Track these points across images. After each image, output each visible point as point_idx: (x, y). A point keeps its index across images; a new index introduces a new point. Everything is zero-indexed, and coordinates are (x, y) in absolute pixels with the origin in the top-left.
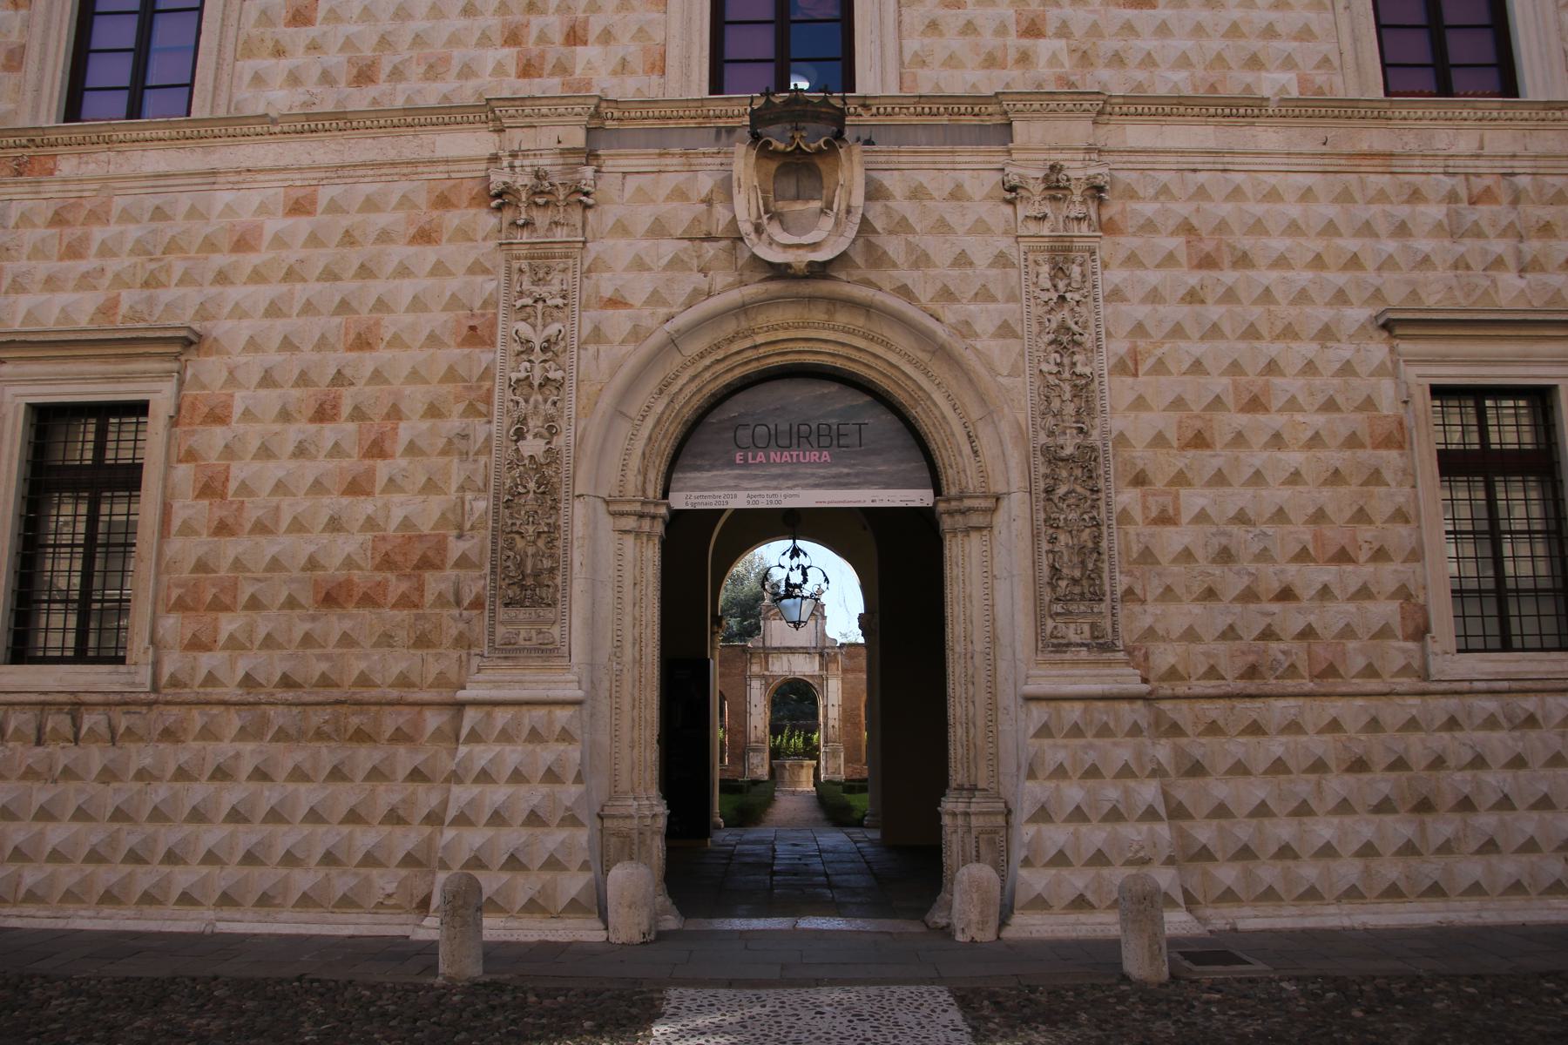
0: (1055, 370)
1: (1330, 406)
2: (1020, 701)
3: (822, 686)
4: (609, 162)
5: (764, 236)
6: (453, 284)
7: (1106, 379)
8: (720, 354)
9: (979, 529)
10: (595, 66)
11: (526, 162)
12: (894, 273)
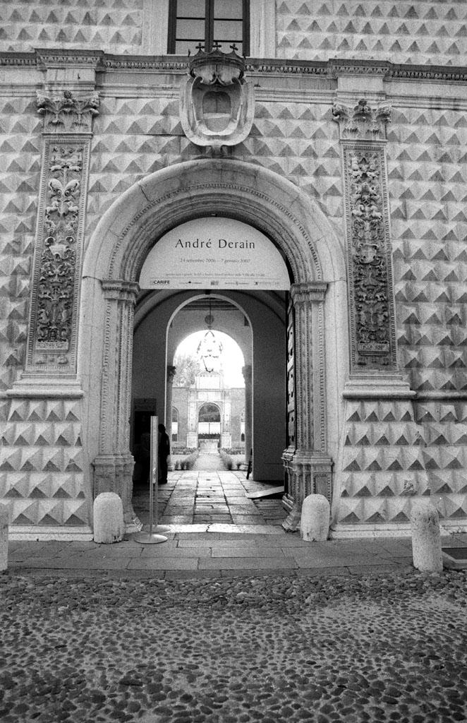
4: (108, 91)
7: (389, 219)
8: (170, 201)
9: (317, 302)
11: (60, 88)
12: (271, 158)
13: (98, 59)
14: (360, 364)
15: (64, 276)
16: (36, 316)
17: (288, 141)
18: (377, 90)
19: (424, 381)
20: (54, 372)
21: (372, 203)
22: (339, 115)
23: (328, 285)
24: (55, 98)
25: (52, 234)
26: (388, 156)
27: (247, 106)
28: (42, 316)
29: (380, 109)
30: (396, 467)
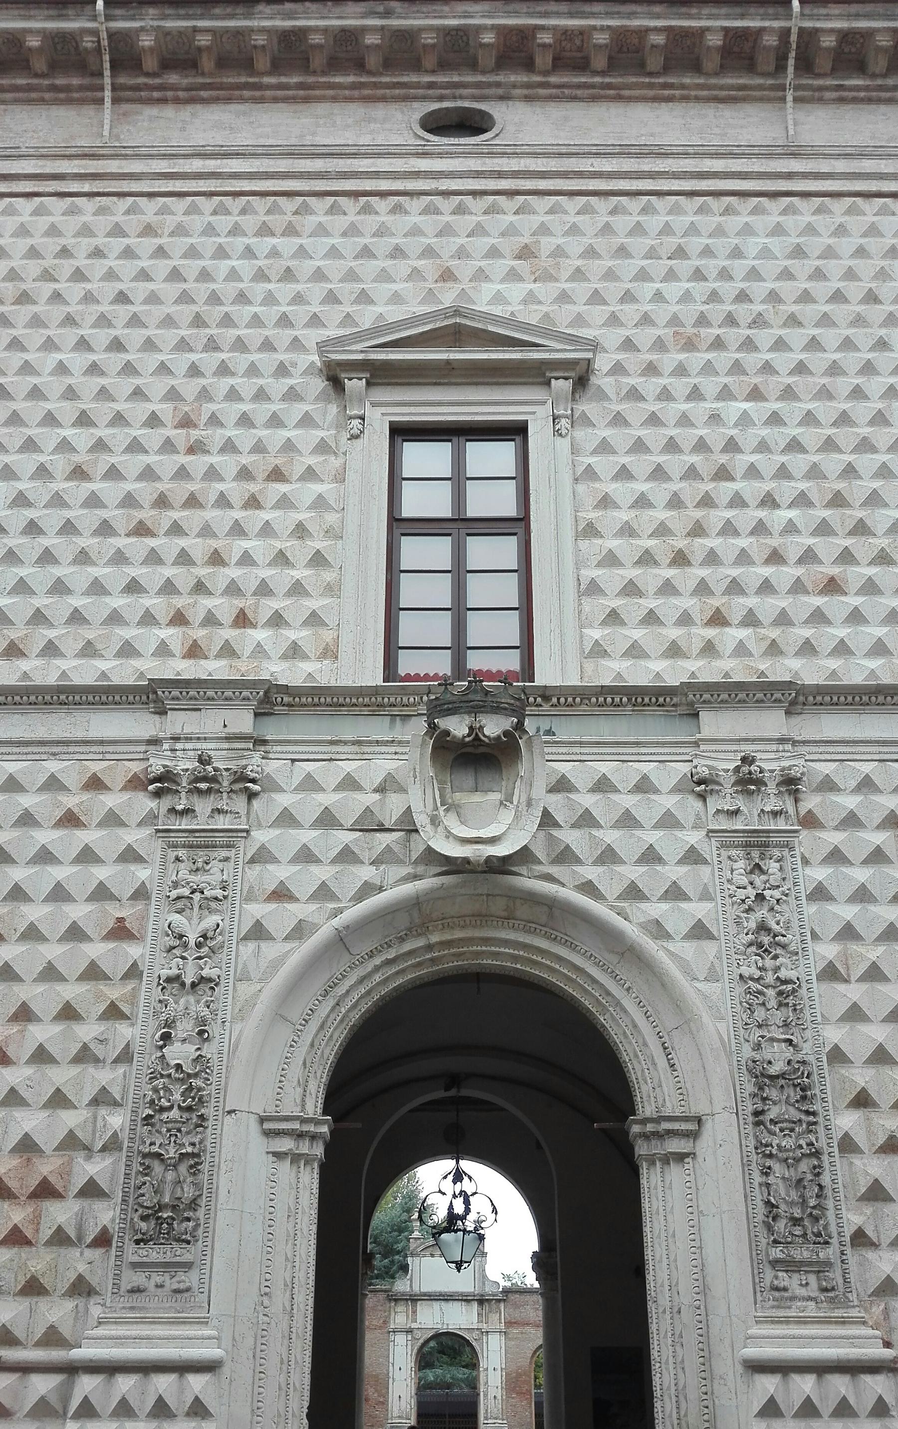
2: (740, 1369)
4: (279, 748)
5: (440, 829)
8: (391, 954)
9: (681, 1157)
11: (189, 746)
12: (578, 869)
13: (261, 693)
15: (189, 1109)
17: (610, 836)
18: (777, 735)
21: (779, 951)
22: (702, 786)
23: (699, 1120)
24: (179, 763)
29: (783, 769)
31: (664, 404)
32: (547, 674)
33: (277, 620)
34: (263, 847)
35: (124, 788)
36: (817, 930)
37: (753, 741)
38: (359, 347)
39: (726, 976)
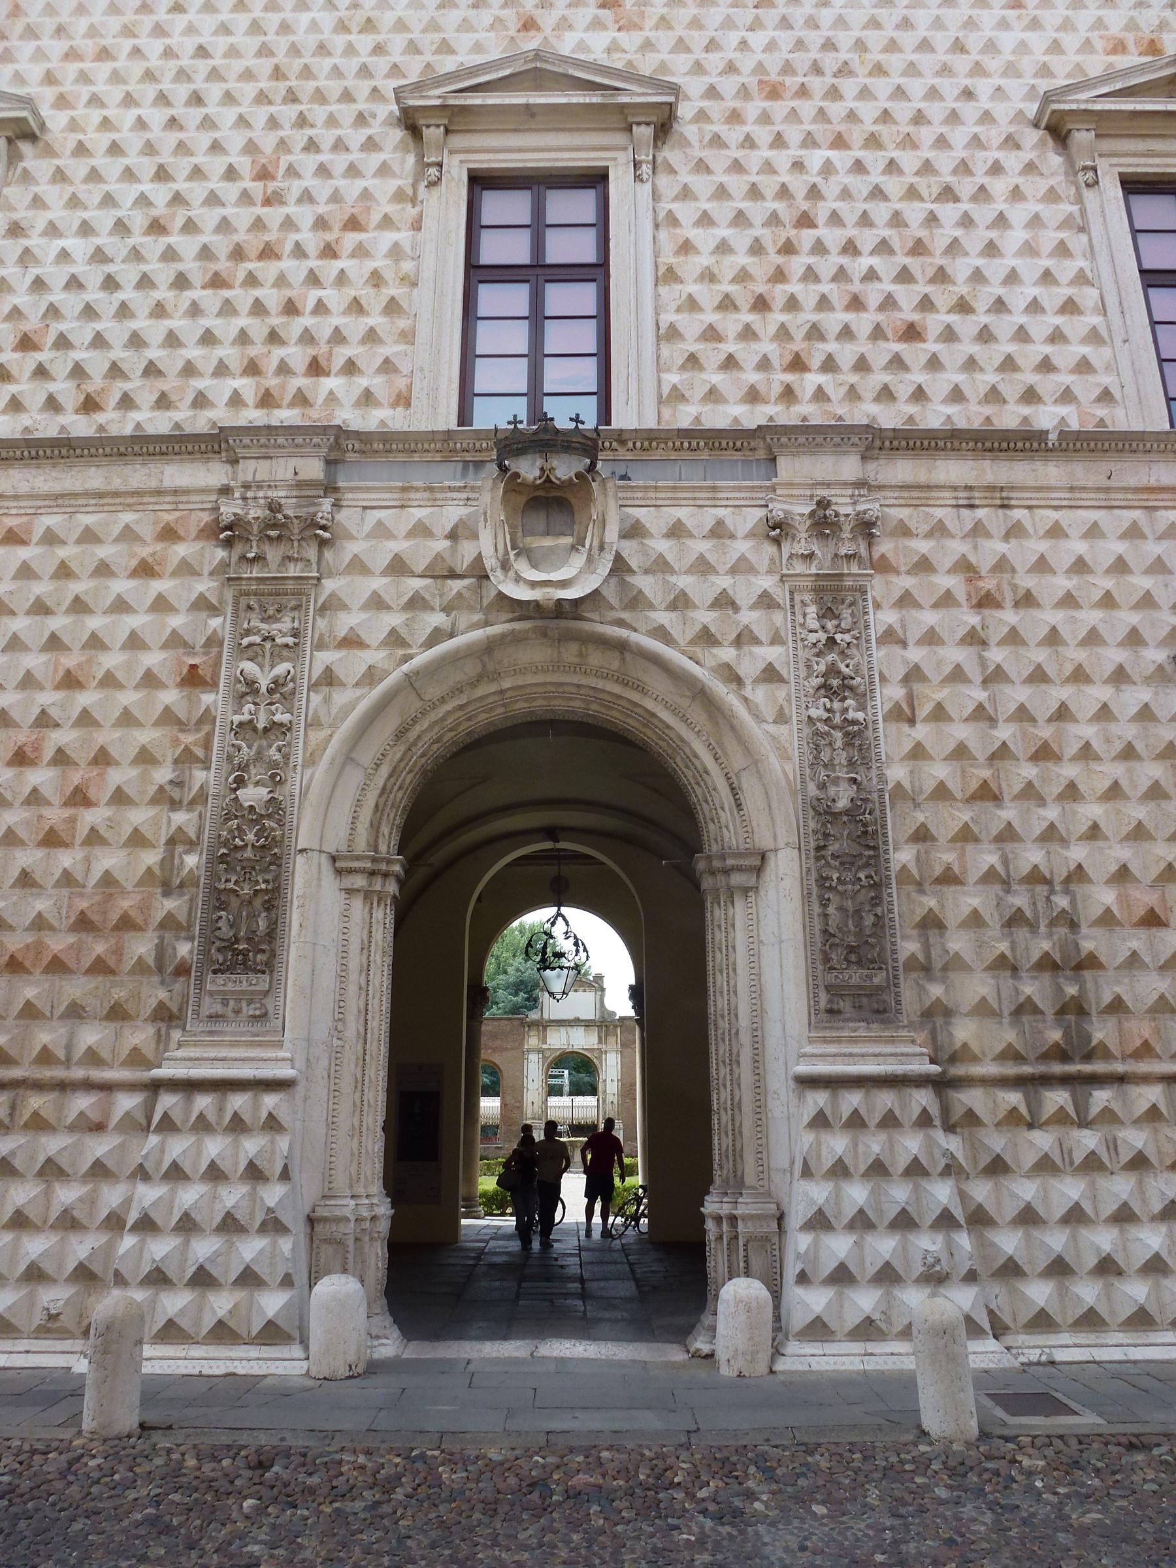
0: (825, 715)
1: (1129, 753)
3: (600, 1058)
4: (350, 496)
5: (511, 574)
6: (177, 621)
7: (881, 725)
8: (463, 700)
9: (746, 891)
10: (341, 402)
11: (261, 494)
12: (652, 615)
14: (830, 1011)
15: (263, 846)
16: (211, 926)
17: (684, 582)
19: (958, 1045)
20: (242, 1034)
23: (763, 857)
25: (243, 767)
26: (875, 601)
27: (604, 521)
28: (220, 924)
30: (904, 1222)
31: (748, 151)
32: (624, 418)
33: (351, 368)
34: (332, 595)
35: (198, 538)
36: (886, 672)
37: (828, 485)
38: (437, 92)
39: (795, 719)
